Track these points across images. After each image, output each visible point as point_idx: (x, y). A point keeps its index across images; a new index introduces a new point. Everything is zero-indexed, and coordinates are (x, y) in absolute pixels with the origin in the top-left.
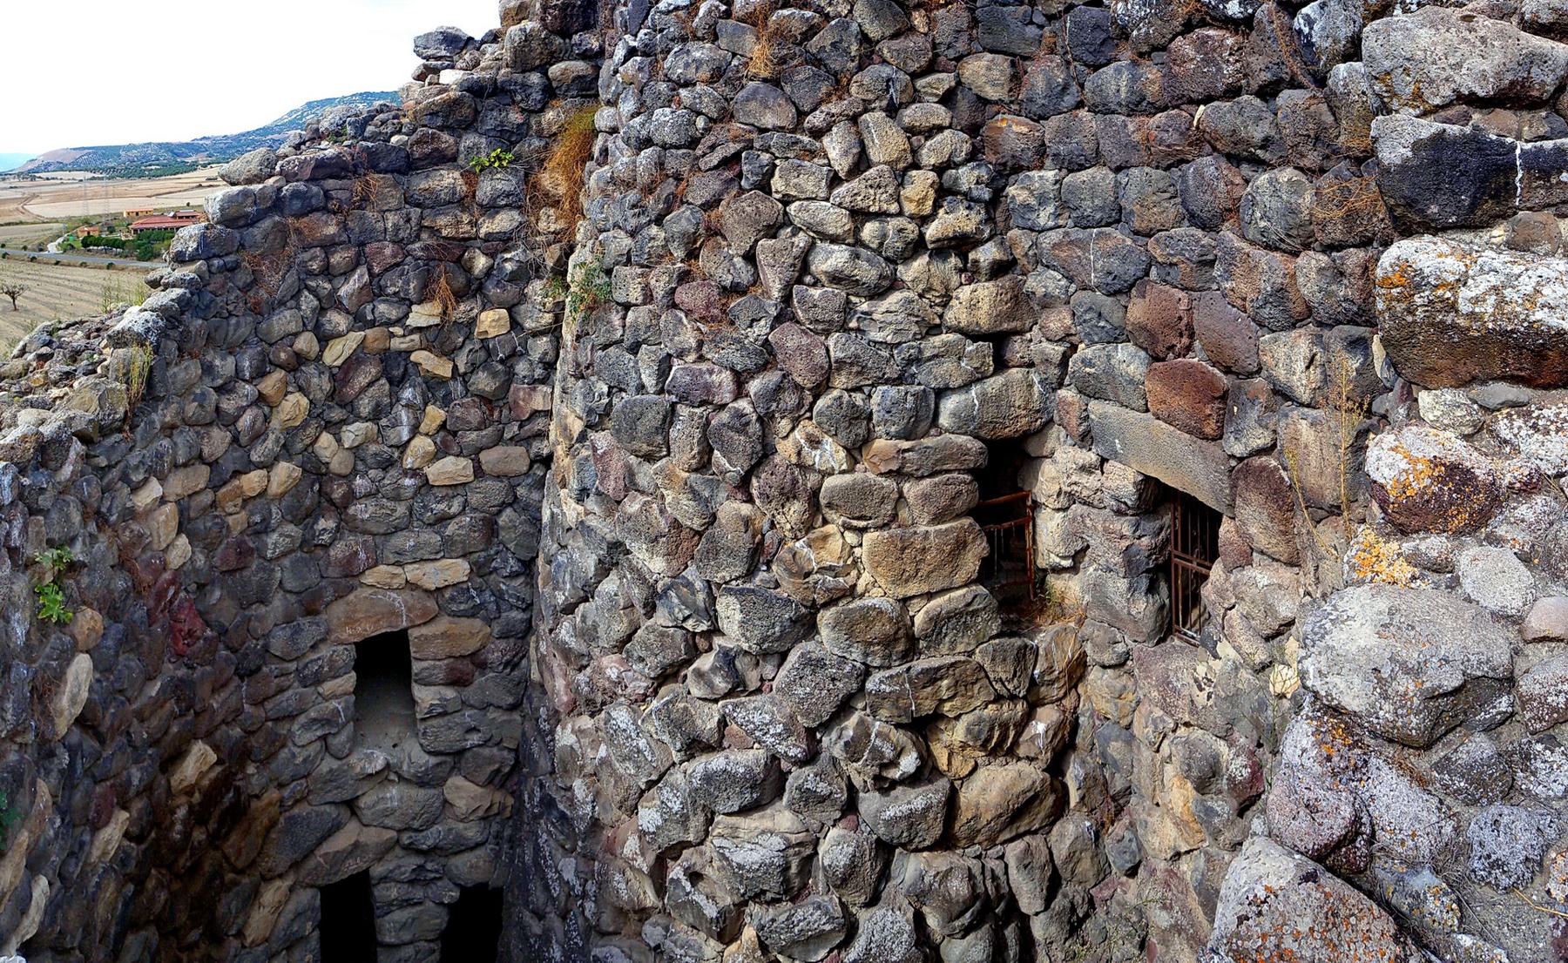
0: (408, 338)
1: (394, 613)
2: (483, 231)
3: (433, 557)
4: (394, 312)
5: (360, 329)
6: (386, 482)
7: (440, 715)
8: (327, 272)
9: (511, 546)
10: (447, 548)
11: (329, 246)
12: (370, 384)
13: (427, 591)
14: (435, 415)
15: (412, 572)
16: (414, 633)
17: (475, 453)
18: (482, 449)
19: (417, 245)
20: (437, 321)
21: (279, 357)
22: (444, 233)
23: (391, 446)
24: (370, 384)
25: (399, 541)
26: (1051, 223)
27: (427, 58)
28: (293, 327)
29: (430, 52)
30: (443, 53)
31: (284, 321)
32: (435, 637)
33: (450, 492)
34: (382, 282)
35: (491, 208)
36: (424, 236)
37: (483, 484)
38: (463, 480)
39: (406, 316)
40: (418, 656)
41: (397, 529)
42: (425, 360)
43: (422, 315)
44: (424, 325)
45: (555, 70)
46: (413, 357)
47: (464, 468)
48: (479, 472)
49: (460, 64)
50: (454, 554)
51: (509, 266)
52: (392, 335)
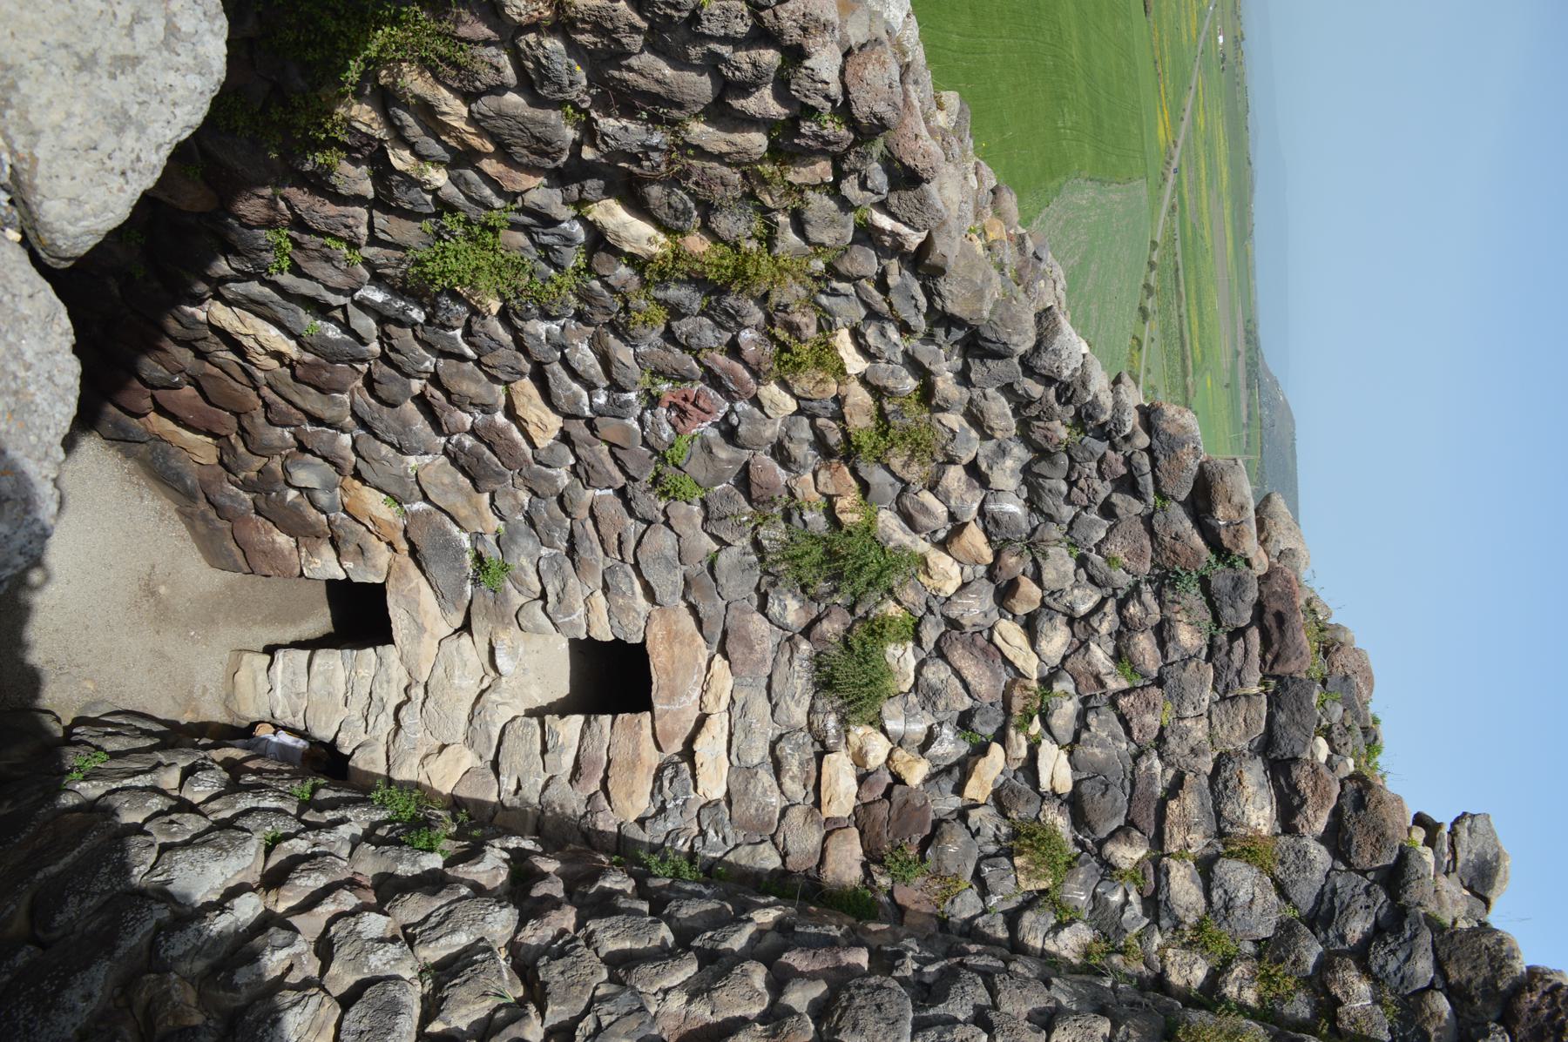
1: (672, 695)
4: (1060, 722)
7: (544, 743)
10: (742, 772)
11: (1162, 634)
13: (690, 741)
14: (916, 773)
22: (1173, 804)
25: (761, 706)
27: (1453, 833)
29: (1463, 833)
30: (1462, 856)
33: (812, 782)
42: (993, 766)
43: (1056, 769)
46: (996, 748)
49: (1443, 880)
50: (733, 777)
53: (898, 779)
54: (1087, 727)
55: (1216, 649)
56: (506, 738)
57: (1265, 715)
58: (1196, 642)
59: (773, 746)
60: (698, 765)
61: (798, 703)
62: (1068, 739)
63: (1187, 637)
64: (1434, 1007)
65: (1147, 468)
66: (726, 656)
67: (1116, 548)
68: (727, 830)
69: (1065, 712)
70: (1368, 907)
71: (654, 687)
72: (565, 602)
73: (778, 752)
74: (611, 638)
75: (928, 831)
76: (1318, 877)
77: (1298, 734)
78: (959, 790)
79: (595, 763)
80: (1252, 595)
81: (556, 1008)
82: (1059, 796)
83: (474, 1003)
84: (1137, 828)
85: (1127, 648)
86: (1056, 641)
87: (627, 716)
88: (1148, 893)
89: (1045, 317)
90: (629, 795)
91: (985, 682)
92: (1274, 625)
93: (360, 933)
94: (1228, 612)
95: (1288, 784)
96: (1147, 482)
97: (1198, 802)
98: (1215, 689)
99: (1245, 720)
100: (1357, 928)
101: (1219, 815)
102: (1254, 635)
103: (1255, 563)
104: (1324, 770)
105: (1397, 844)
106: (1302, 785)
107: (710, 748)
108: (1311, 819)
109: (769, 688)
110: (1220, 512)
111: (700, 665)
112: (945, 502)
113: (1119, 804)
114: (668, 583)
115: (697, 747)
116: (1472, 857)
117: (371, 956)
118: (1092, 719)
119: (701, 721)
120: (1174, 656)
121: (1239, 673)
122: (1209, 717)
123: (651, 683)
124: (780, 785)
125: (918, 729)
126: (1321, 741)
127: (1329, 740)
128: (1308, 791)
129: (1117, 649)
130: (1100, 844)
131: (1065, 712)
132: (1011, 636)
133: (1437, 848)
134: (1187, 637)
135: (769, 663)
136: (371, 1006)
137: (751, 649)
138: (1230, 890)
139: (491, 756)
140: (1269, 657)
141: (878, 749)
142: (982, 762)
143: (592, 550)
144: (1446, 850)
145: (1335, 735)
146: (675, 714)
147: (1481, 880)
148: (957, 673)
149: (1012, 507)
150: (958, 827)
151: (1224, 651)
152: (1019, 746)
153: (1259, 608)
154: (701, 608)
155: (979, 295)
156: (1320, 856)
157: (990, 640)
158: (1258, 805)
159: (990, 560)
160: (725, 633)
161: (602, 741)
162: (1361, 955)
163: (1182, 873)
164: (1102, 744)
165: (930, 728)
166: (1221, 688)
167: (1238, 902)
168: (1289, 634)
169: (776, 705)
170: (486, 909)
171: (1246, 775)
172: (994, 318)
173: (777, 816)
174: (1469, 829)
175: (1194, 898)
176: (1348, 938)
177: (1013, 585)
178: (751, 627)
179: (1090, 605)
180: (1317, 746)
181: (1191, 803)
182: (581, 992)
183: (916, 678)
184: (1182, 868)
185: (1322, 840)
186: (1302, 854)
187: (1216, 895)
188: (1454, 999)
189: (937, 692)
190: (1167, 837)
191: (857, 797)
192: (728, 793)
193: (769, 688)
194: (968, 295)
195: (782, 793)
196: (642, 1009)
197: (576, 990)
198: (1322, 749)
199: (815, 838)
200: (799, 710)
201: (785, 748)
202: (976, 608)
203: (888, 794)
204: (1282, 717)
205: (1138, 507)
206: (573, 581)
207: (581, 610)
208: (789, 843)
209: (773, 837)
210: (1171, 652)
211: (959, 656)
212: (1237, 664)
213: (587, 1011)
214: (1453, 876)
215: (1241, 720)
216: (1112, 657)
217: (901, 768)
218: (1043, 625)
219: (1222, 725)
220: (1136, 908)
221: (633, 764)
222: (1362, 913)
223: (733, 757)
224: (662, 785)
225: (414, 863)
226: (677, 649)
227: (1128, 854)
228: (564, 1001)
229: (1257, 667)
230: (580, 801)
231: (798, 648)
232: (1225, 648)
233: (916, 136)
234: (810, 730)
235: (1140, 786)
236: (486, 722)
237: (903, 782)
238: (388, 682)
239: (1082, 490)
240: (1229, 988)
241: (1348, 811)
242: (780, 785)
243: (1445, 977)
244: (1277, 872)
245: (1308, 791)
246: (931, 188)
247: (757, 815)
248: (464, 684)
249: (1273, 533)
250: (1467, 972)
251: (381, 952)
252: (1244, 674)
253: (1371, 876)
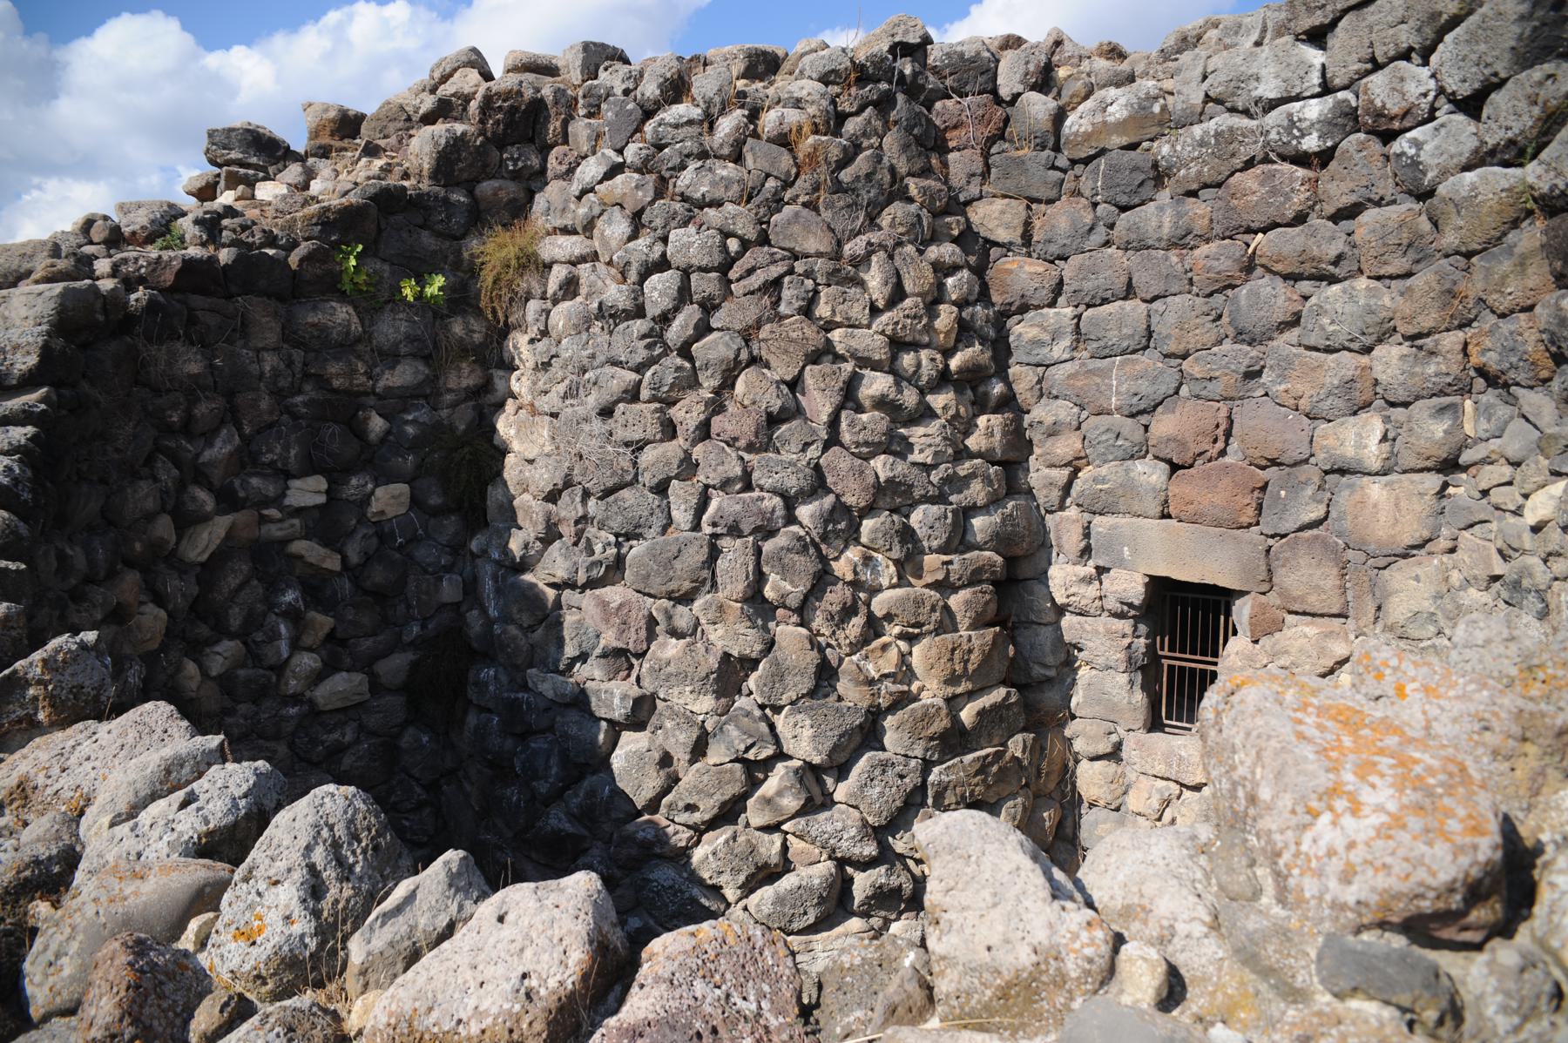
0: (286, 524)
2: (381, 384)
8: (187, 428)
9: (416, 772)
12: (241, 587)
14: (323, 622)
19: (299, 399)
20: (322, 499)
26: (1066, 356)
28: (150, 504)
31: (143, 495)
36: (308, 387)
38: (357, 699)
39: (284, 495)
42: (308, 549)
43: (308, 491)
45: (486, 187)
48: (376, 687)
52: (264, 520)
164: (286, 448)
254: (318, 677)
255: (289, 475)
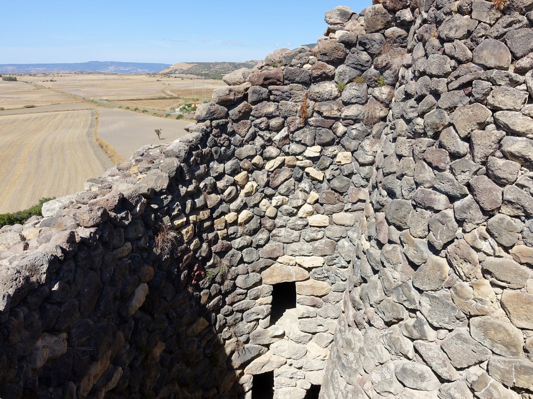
1: (291, 275)
3: (308, 254)
4: (298, 149)
5: (283, 156)
6: (290, 221)
7: (306, 317)
9: (343, 255)
11: (270, 116)
12: (286, 180)
13: (305, 268)
14: (314, 195)
15: (299, 260)
16: (297, 284)
17: (330, 214)
18: (334, 213)
19: (312, 119)
21: (244, 165)
22: (325, 114)
23: (293, 207)
24: (286, 180)
25: (293, 246)
27: (331, 24)
29: (331, 20)
30: (338, 21)
31: (247, 150)
32: (307, 286)
33: (318, 229)
34: (294, 136)
35: (346, 104)
36: (315, 114)
37: (332, 228)
39: (304, 151)
40: (299, 293)
41: (294, 241)
42: (313, 172)
43: (313, 151)
44: (312, 156)
47: (325, 220)
48: (332, 223)
49: (346, 28)
50: (317, 254)
51: (354, 132)
53: (317, 201)
54: (300, 141)
55: (276, 100)
56: (305, 330)
57: (296, 84)
58: (273, 106)
59: (308, 242)
60: (313, 266)
61: (292, 234)
62: (304, 147)
63: (270, 108)
64: (390, 33)
65: (217, 121)
66: (277, 258)
67: (243, 131)
68: (334, 256)
69: (294, 148)
70: (358, 53)
71: (287, 281)
72: (260, 312)
73: (309, 240)
74: (271, 296)
75: (333, 191)
76: (348, 69)
77: (303, 74)
78: (321, 182)
79: (313, 300)
80: (258, 88)
81: (401, 315)
82: (322, 150)
83: (401, 342)
84: (332, 126)
85: (275, 128)
86: (272, 151)
87: (297, 290)
88: (351, 122)
89: (167, 155)
90: (323, 288)
91: (285, 173)
92: (268, 81)
93: (379, 382)
94: (264, 96)
95: (319, 77)
96: (221, 121)
97: (324, 106)
98: (288, 100)
99: (298, 91)
100: (365, 56)
101: (328, 100)
102: (271, 87)
103: (248, 86)
104: (314, 66)
105: (338, 43)
106: (319, 73)
107: (307, 262)
108: (330, 70)
109: (288, 243)
110: (232, 97)
111: (280, 266)
112: (228, 186)
113: (324, 131)
114: (254, 277)
115: (307, 267)
116: (339, 18)
117: (387, 378)
118: (297, 139)
119: (300, 266)
120: (277, 113)
121: (284, 93)
122: (297, 102)
123: (286, 282)
124: (319, 239)
125: (301, 195)
126: (305, 66)
127: (304, 64)
128: (321, 71)
129: (275, 131)
130: (338, 137)
131: (294, 148)
132: (270, 165)
133: (336, 29)
134: (270, 108)
135: (279, 243)
136: (404, 378)
137: (275, 249)
138: (352, 96)
139: (311, 335)
140: (278, 83)
141: (307, 208)
142: (311, 174)
143: (242, 304)
144: (337, 26)
145: (302, 62)
146: (296, 274)
147: (347, 16)
148: (283, 183)
149: (229, 165)
150: (331, 182)
151: (276, 97)
152: (306, 162)
153: (263, 85)
154: (261, 266)
155: (160, 177)
156: (341, 68)
157: (272, 172)
158: (325, 87)
159: (246, 172)
160: (270, 258)
161: (306, 298)
162: (372, 56)
163: (347, 112)
164: (306, 136)
165: (301, 191)
166: (288, 98)
167: (356, 94)
168: (271, 76)
169: (293, 241)
170: (368, 338)
171: (316, 91)
172: (168, 172)
173: (329, 240)
174: (330, 19)
175: (354, 108)
176: (368, 60)
177: (254, 164)
178: (268, 250)
179: (261, 139)
180: (306, 68)
181: (325, 109)
182: (396, 306)
183: (285, 195)
184: (345, 111)
185: (336, 67)
186: (340, 74)
187: (354, 101)
188: (388, 27)
189: (289, 189)
190: (335, 116)
191: (323, 214)
192: (322, 256)
193: (288, 243)
194: (160, 181)
195: (321, 238)
196: (400, 286)
197: (395, 308)
198: (307, 66)
199: (335, 227)
200: (295, 233)
201: (307, 238)
202: (262, 176)
203: (322, 205)
204: (297, 79)
205: (230, 125)
206: (252, 310)
207: (262, 306)
208: (338, 236)
209: (337, 241)
210: (276, 114)
211: (277, 182)
212: (280, 93)
213: (402, 304)
214: (345, 24)
215: (298, 92)
216: (278, 133)
217: (313, 200)
218: (267, 154)
219: (300, 98)
220: (357, 126)
221: (312, 287)
222: (360, 55)
223: (310, 254)
224: (320, 278)
225: (352, 362)
226: (274, 274)
227: (341, 129)
228: (399, 312)
229: (281, 87)
230: (325, 304)
231: (275, 234)
232: (275, 96)
233: (107, 200)
234: (301, 230)
235: (318, 124)
236: (300, 337)
237: (318, 199)
238: (286, 372)
239: (224, 142)
240: (383, 97)
241: (327, 58)
242: (319, 239)
243: (380, 30)
244: (346, 82)
245: (321, 71)
246: (126, 194)
247: (329, 246)
248: (287, 346)
249: (238, 80)
250: (379, 23)
251: (385, 374)
252: (283, 91)
253: (348, 51)
254: (311, 214)
255: (308, 146)
